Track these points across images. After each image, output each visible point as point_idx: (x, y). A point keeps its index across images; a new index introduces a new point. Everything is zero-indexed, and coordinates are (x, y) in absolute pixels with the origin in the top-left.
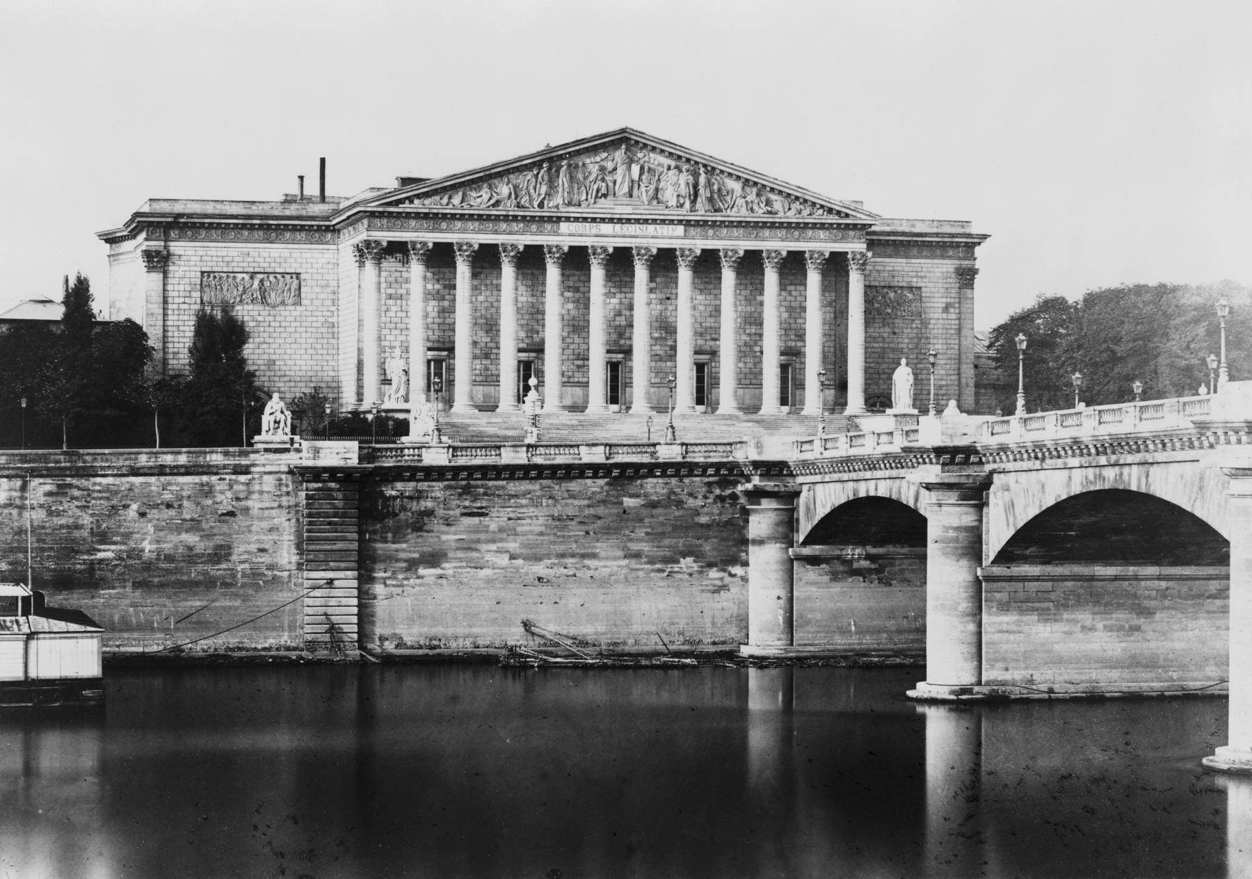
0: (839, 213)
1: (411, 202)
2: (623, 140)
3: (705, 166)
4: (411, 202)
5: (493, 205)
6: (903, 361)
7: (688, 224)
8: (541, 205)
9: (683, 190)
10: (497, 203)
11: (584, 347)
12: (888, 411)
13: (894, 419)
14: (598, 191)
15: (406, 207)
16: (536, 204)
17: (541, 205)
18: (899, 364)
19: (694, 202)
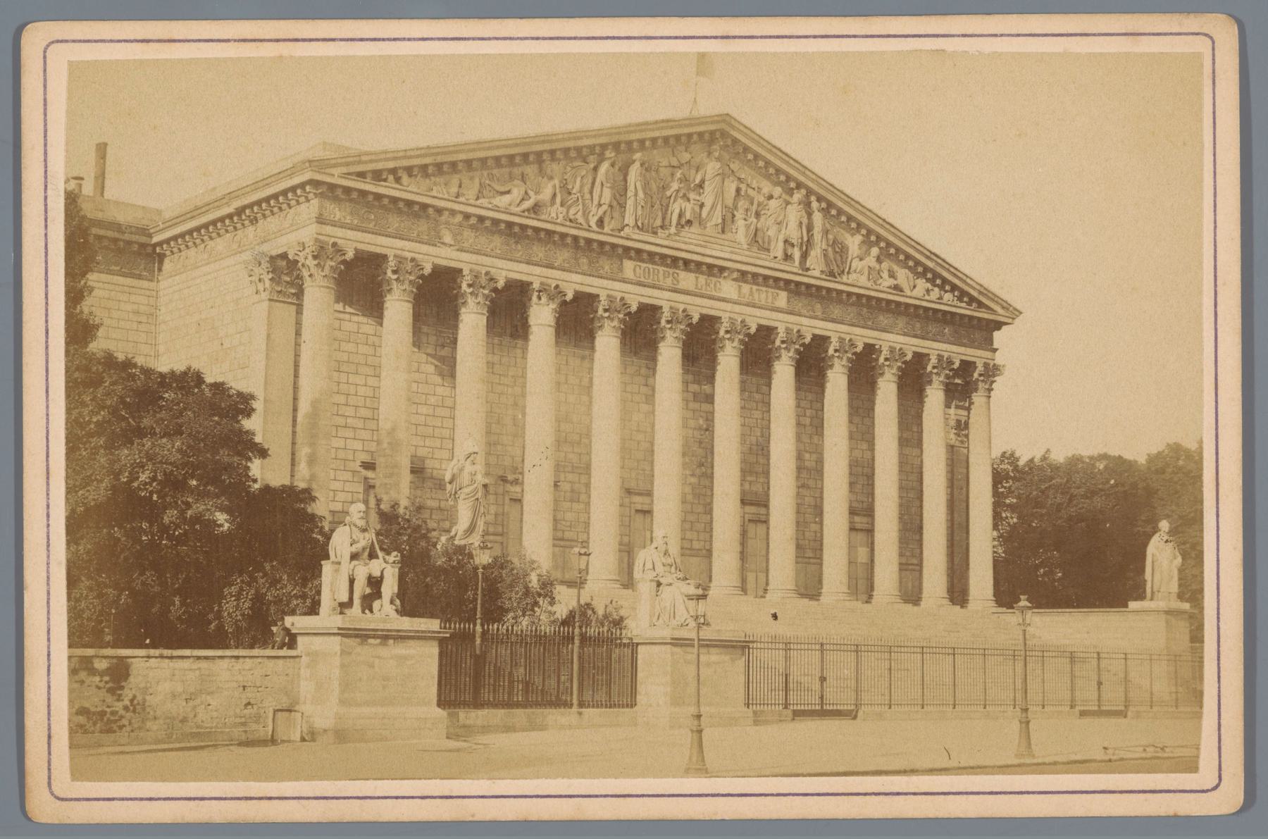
0: (972, 299)
1: (398, 180)
3: (819, 199)
5: (528, 210)
6: (1164, 525)
7: (795, 289)
8: (600, 222)
9: (793, 232)
10: (536, 209)
11: (868, 455)
12: (1133, 605)
13: (1163, 616)
14: (680, 216)
15: (388, 189)
16: (593, 222)
18: (1155, 530)
19: (804, 256)
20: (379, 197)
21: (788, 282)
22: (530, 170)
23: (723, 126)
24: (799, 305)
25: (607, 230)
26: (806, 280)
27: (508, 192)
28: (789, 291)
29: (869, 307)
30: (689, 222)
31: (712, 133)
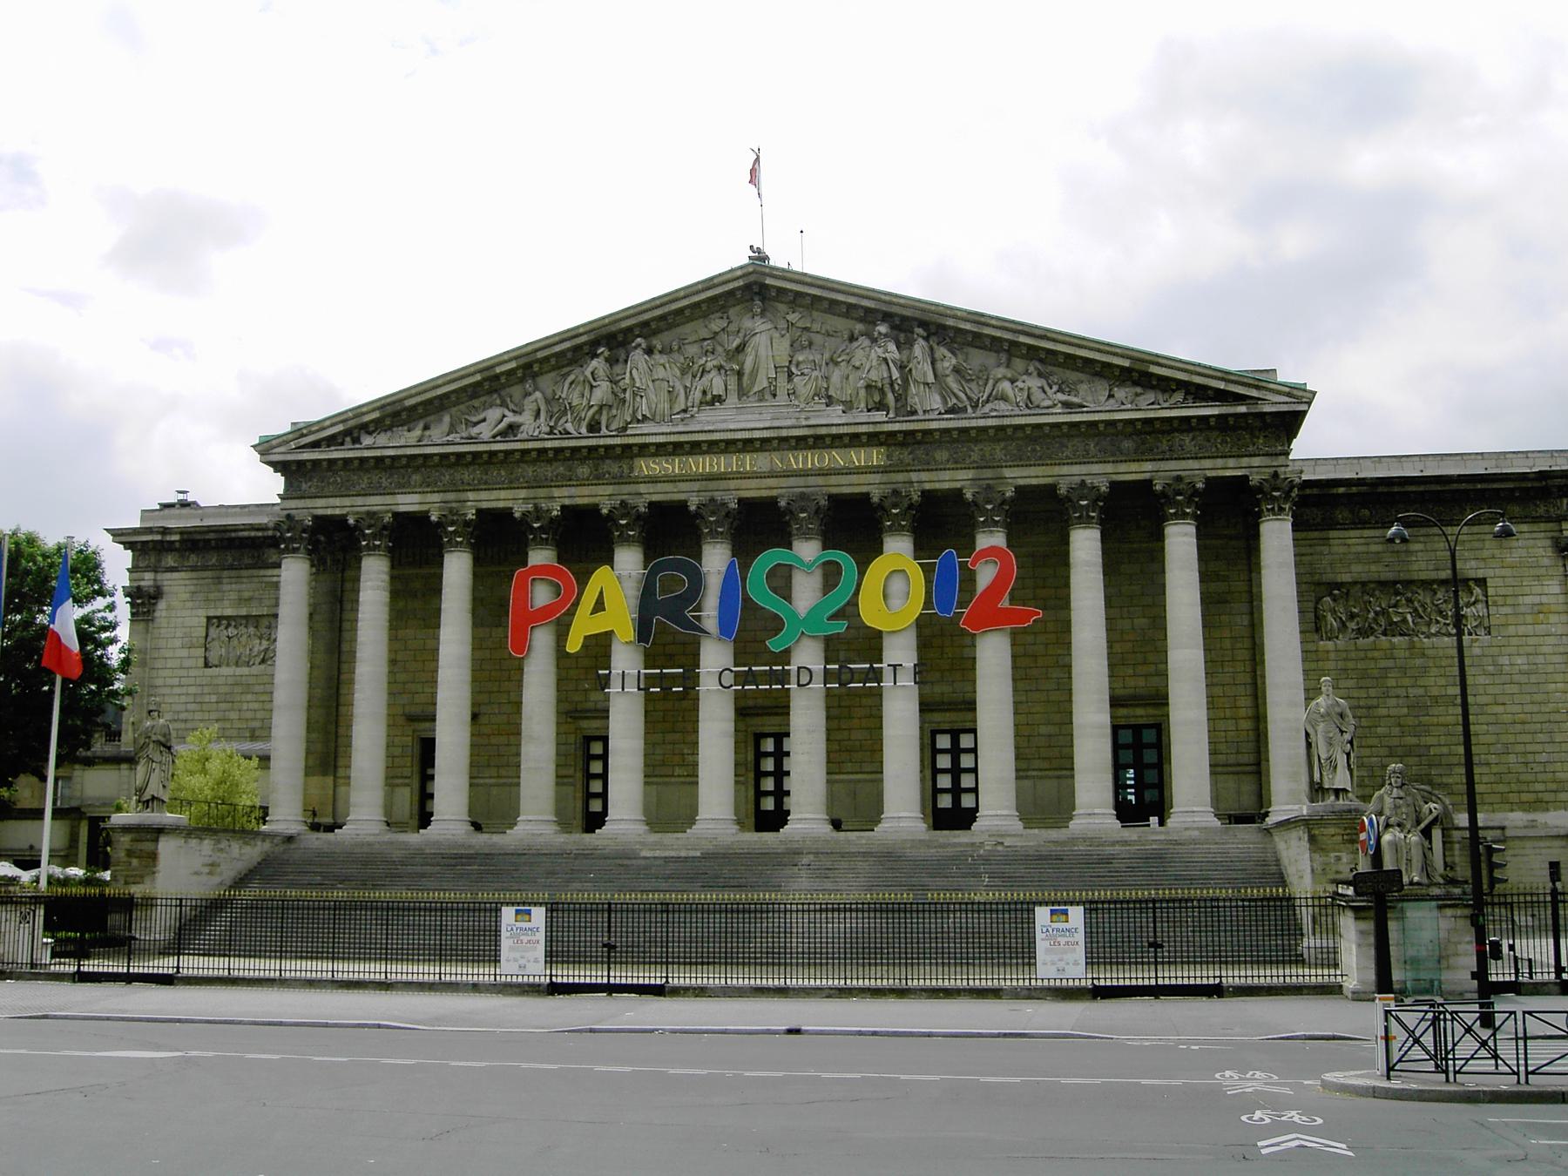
2: (758, 289)
4: (356, 440)
5: (500, 434)
8: (594, 427)
10: (512, 428)
14: (704, 393)
16: (584, 430)
17: (594, 427)
20: (331, 462)
22: (516, 391)
23: (752, 278)
24: (905, 455)
25: (604, 431)
26: (896, 427)
27: (484, 420)
28: (889, 445)
29: (1032, 440)
30: (718, 399)
31: (748, 287)
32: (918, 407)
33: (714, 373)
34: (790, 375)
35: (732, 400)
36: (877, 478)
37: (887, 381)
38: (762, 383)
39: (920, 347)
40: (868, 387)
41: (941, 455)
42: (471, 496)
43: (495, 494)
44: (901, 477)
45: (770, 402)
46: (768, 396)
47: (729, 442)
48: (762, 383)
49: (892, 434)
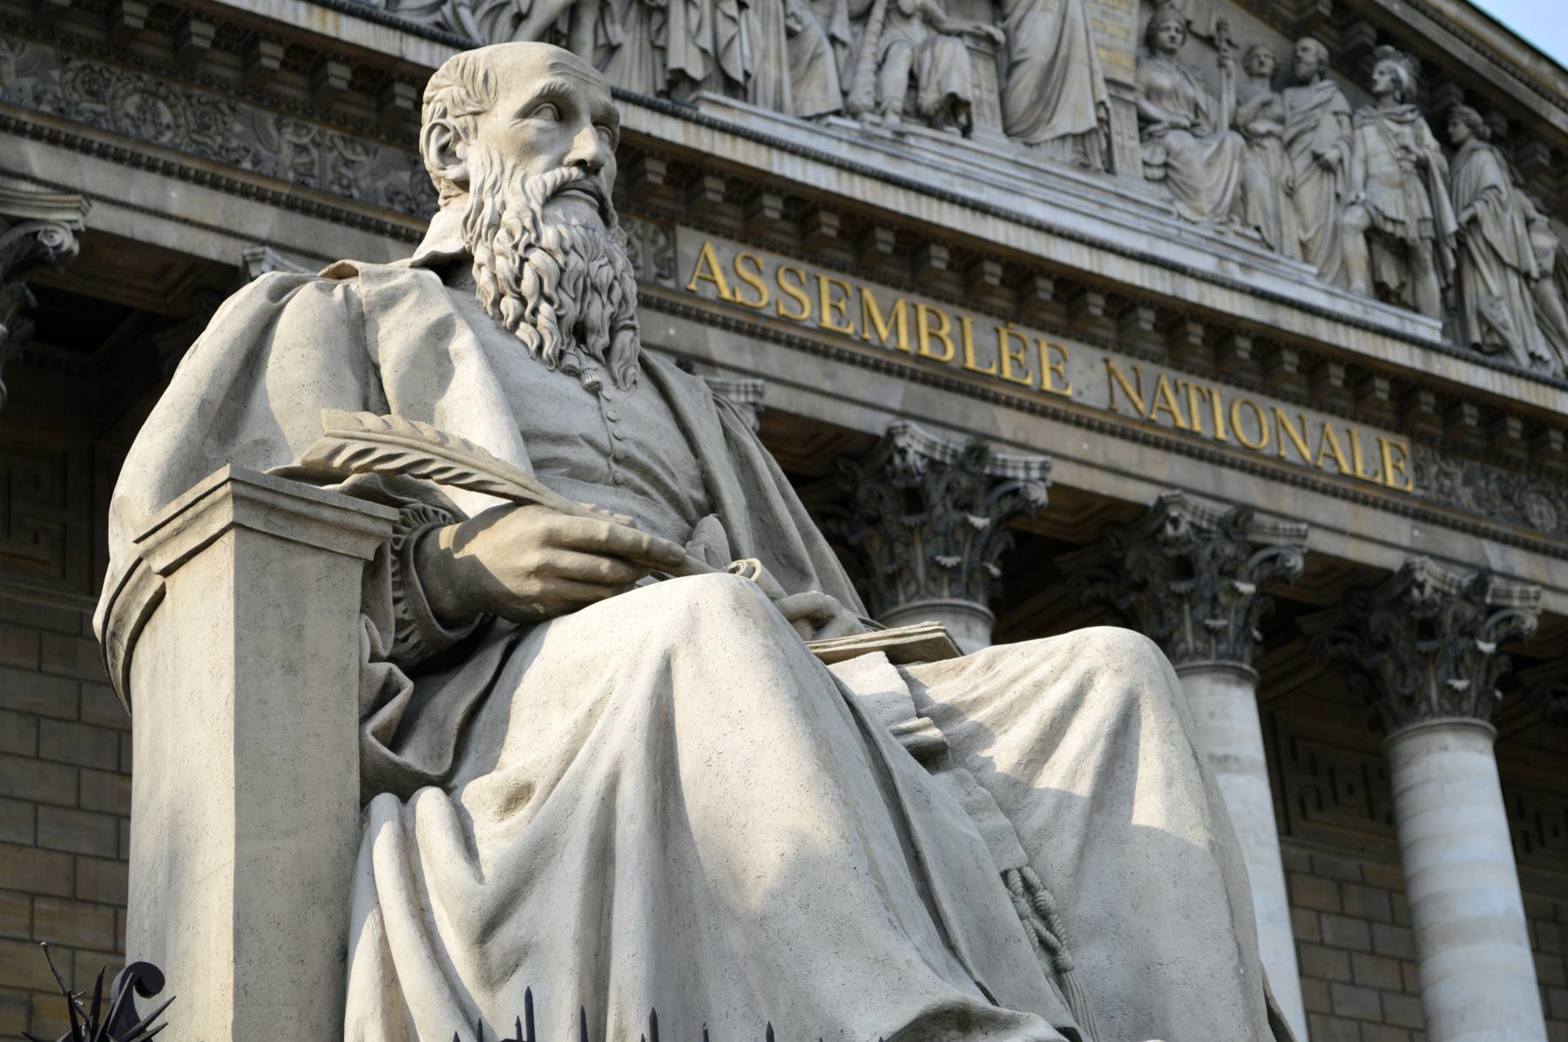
21: (1407, 385)
28: (1416, 438)
32: (1514, 338)
33: (917, 31)
34: (1145, 121)
35: (988, 131)
36: (1402, 530)
37: (1429, 232)
38: (1076, 113)
39: (1487, 166)
40: (1373, 234)
41: (1542, 513)
42: (38, 158)
43: (142, 187)
44: (1460, 545)
45: (1103, 182)
46: (1098, 162)
47: (1023, 272)
48: (1076, 113)
49: (1453, 396)
